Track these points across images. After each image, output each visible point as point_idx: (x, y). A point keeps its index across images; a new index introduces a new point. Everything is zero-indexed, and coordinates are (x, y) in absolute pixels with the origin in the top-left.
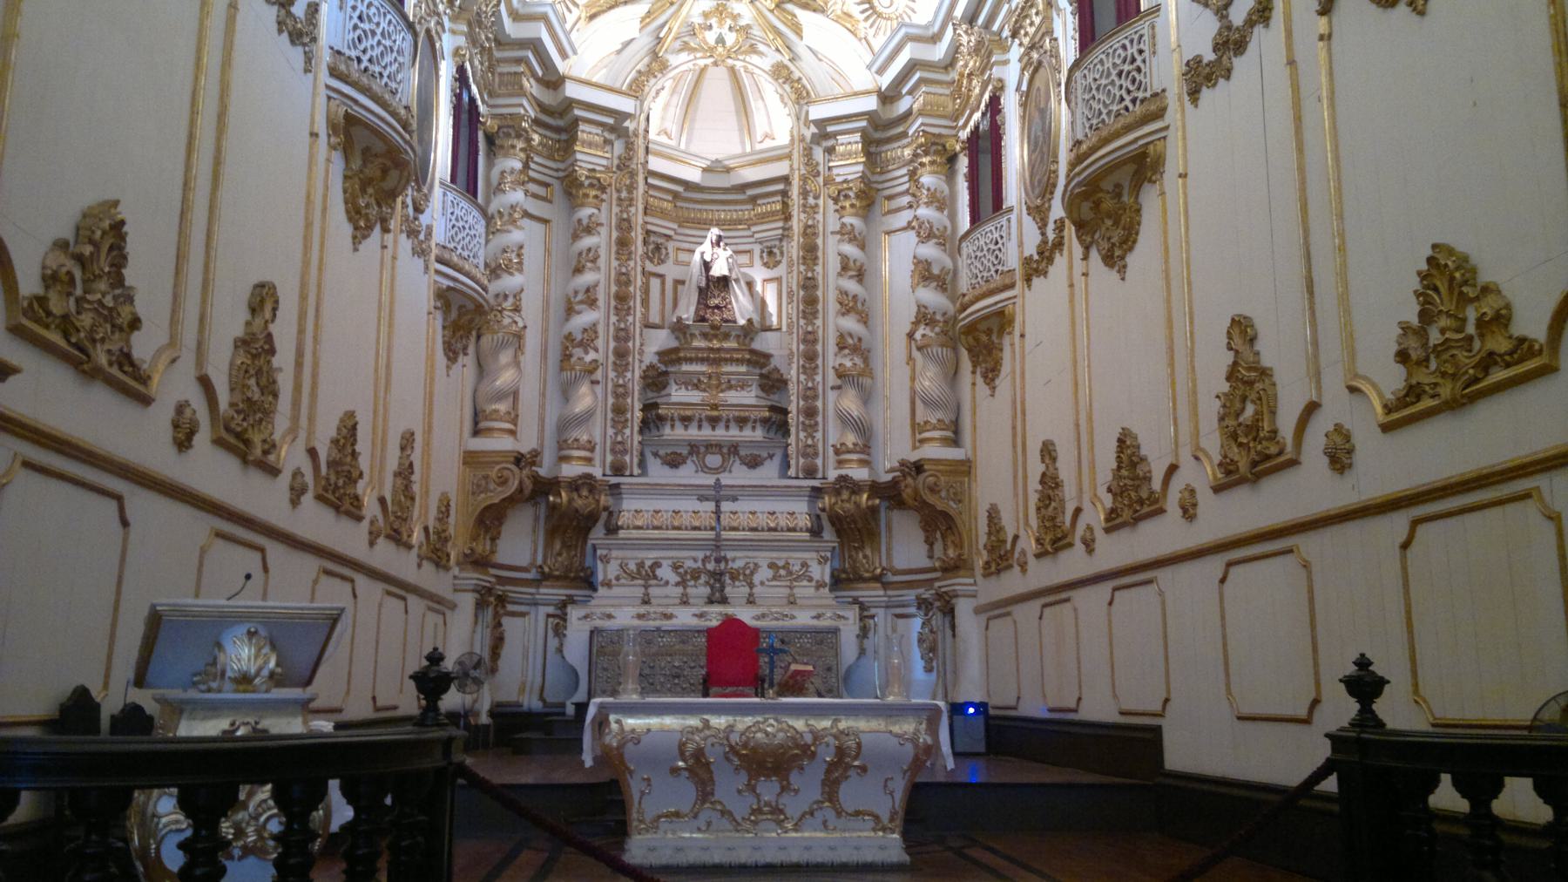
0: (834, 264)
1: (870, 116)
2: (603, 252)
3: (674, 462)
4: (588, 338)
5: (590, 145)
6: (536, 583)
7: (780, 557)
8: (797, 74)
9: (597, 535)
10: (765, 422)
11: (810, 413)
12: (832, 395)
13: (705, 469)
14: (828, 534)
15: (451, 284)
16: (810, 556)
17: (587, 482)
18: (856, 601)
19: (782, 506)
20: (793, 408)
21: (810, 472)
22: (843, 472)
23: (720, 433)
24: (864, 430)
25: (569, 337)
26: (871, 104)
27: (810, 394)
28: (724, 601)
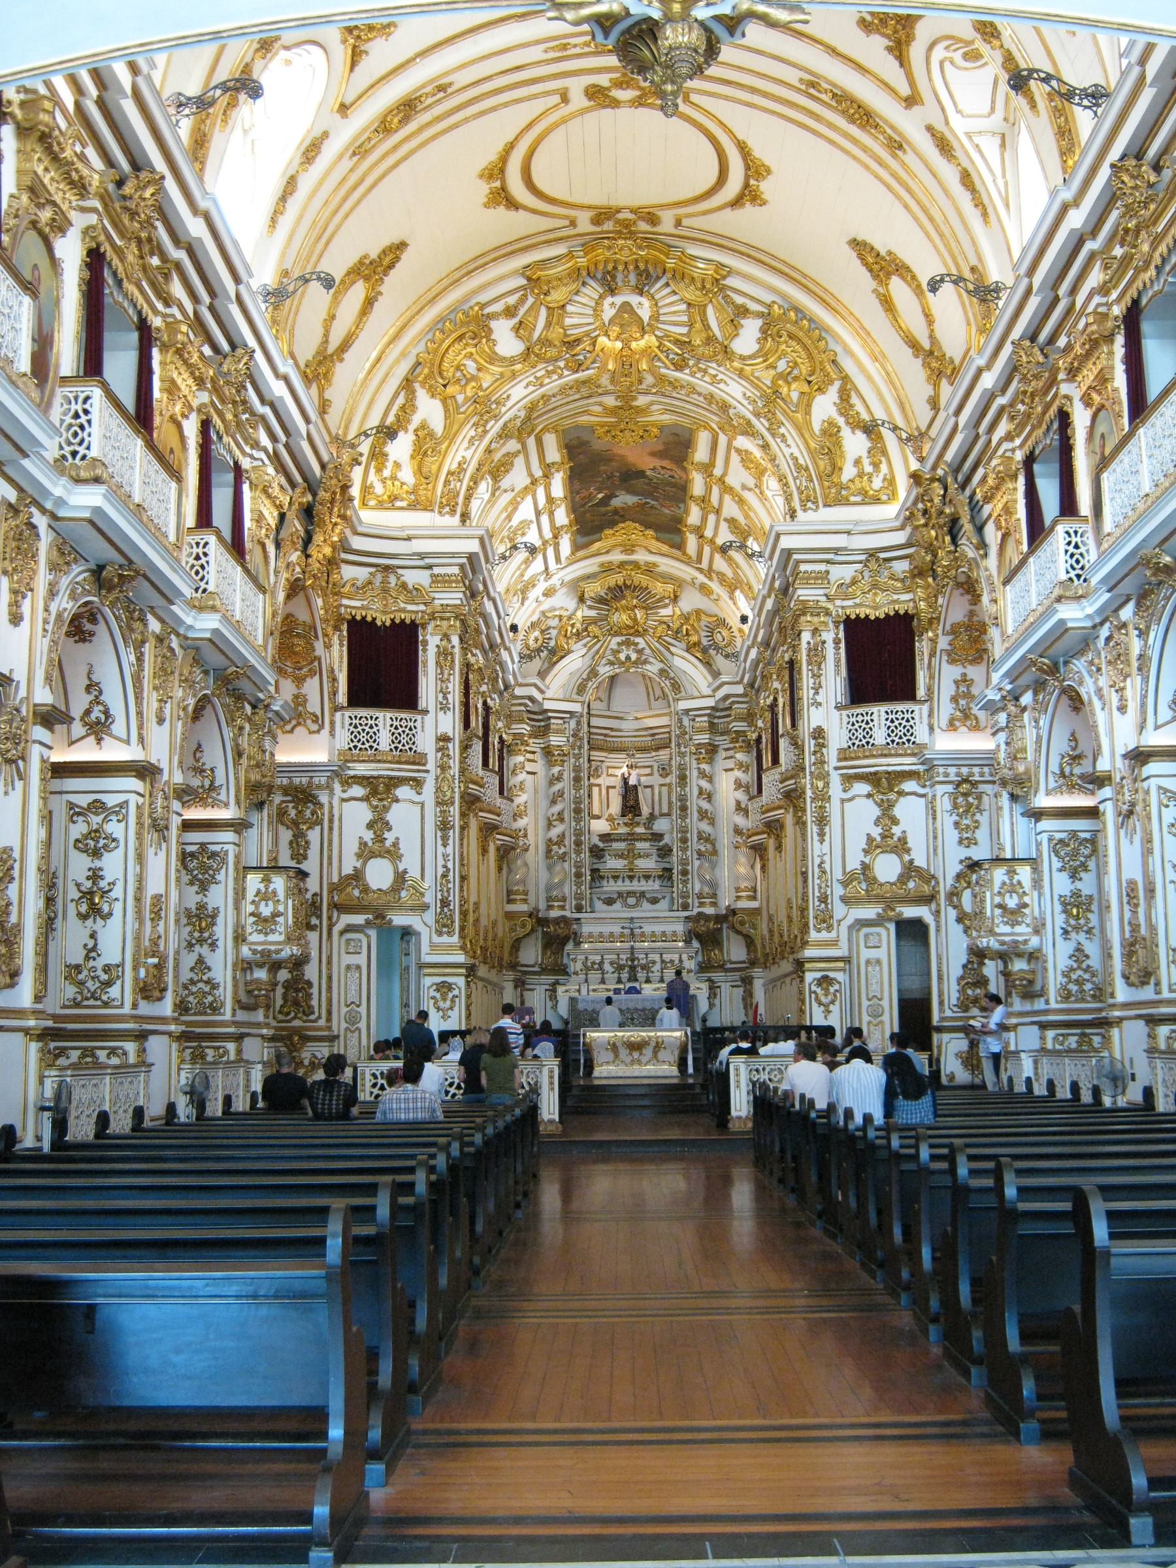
0: (696, 792)
1: (712, 708)
3: (609, 902)
5: (557, 732)
9: (569, 946)
10: (660, 877)
11: (685, 873)
14: (696, 944)
18: (709, 980)
23: (636, 886)
24: (713, 885)
25: (550, 840)
26: (711, 702)
27: (684, 862)
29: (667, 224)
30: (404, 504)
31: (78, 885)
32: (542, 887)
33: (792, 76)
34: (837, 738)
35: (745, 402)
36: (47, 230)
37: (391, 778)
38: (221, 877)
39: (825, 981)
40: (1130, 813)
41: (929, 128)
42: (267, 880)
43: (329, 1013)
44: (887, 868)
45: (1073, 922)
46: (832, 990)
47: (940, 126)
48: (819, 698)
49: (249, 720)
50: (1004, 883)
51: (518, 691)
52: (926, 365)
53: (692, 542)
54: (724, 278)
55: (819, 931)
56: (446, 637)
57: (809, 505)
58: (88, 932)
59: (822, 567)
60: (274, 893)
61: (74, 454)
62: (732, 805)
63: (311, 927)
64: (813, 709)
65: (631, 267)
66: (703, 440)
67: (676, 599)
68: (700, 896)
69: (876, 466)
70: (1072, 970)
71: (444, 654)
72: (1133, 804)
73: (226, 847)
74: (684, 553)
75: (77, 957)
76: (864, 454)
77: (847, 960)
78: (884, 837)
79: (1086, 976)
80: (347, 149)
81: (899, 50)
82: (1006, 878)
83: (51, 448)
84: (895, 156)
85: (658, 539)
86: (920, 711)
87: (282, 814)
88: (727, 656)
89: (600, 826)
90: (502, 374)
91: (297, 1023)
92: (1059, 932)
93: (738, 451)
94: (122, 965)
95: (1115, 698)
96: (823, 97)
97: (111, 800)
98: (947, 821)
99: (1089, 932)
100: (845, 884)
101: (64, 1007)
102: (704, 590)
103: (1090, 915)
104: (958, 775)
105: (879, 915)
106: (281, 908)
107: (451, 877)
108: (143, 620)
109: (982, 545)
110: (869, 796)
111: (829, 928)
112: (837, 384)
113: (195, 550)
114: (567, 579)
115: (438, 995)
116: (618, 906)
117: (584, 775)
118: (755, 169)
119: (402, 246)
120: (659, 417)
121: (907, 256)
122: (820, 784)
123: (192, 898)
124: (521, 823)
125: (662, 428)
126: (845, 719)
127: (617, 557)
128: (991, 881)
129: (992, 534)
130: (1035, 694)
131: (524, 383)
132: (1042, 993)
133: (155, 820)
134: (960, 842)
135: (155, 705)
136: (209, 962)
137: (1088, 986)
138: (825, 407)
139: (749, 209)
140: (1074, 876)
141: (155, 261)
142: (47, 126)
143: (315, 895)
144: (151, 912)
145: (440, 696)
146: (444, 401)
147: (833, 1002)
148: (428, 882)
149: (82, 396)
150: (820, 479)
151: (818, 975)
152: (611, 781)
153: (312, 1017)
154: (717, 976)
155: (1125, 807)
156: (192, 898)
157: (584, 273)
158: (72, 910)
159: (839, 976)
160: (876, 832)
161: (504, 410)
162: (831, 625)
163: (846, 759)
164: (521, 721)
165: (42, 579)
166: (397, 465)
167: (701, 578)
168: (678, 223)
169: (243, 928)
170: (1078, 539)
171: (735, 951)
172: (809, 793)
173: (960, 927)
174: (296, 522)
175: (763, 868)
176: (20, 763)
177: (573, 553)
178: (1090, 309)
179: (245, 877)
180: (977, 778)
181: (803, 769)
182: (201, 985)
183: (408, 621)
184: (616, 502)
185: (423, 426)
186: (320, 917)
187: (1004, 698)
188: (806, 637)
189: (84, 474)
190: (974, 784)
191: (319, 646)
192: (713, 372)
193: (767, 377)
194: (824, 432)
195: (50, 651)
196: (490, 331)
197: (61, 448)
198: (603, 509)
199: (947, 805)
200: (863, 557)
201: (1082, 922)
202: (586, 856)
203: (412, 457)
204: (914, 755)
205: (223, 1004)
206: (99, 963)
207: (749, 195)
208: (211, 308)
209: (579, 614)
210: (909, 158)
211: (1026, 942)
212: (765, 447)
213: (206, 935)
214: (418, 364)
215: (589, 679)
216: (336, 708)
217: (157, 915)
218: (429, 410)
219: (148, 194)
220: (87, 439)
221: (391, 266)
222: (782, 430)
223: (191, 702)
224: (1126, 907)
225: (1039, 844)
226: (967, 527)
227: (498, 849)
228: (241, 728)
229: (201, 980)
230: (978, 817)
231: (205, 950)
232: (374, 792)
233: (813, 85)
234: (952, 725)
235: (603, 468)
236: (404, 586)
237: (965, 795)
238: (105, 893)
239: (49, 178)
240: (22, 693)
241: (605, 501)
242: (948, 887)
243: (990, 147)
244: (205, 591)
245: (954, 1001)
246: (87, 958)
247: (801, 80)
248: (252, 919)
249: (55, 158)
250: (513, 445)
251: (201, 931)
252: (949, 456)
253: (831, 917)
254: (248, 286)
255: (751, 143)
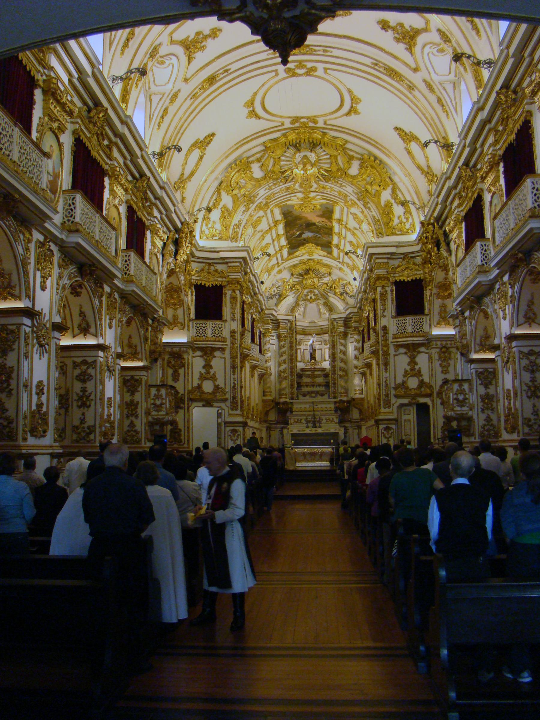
0: (339, 351)
1: (345, 318)
2: (287, 351)
3: (304, 395)
4: (284, 372)
5: (283, 328)
6: (276, 424)
7: (327, 417)
8: (329, 304)
9: (288, 414)
11: (334, 384)
12: (339, 380)
13: (311, 397)
14: (339, 412)
16: (334, 417)
17: (285, 403)
19: (328, 406)
20: (331, 383)
21: (335, 397)
22: (341, 398)
25: (280, 371)
27: (334, 380)
28: (316, 427)
29: (320, 124)
30: (217, 238)
31: (77, 394)
32: (277, 389)
33: (368, 61)
34: (393, 330)
35: (354, 194)
36: (56, 131)
37: (212, 348)
38: (139, 389)
39: (387, 429)
40: (508, 361)
41: (424, 81)
42: (158, 390)
43: (188, 441)
44: (413, 383)
45: (486, 406)
46: (390, 432)
47: (428, 80)
48: (385, 314)
49: (151, 326)
50: (457, 390)
51: (267, 312)
52: (426, 177)
53: (335, 251)
54: (344, 144)
55: (385, 408)
56: (234, 291)
57: (380, 235)
58: (81, 413)
59: (386, 260)
60: (161, 395)
61: (69, 221)
62: (354, 356)
63: (181, 408)
64: (382, 318)
65: (307, 141)
66: (337, 210)
67: (330, 274)
68: (341, 393)
69: (407, 219)
70: (485, 425)
71: (233, 298)
72: (508, 358)
73: (142, 377)
74: (333, 256)
75: (77, 423)
76: (402, 214)
77: (396, 420)
78: (412, 370)
79: (491, 428)
80: (188, 97)
81: (410, 49)
82: (458, 388)
83: (57, 219)
84: (411, 93)
85: (322, 250)
86: (426, 319)
87: (169, 362)
88: (350, 297)
89: (300, 365)
90: (255, 185)
91: (175, 446)
92: (480, 410)
93: (351, 213)
94: (94, 426)
95: (501, 315)
96: (381, 69)
97: (90, 360)
98: (437, 364)
99: (492, 410)
100: (395, 389)
101: (72, 443)
102: (340, 269)
103: (493, 403)
104: (441, 344)
105: (409, 402)
106: (164, 401)
107: (236, 387)
108: (102, 287)
109: (449, 251)
110: (405, 353)
111: (389, 407)
112: (391, 186)
113: (125, 258)
115: (232, 435)
116: (308, 397)
117: (294, 345)
118: (355, 100)
119: (213, 135)
120: (319, 201)
121: (416, 133)
122: (385, 349)
123: (128, 397)
124: (269, 364)
125: (321, 205)
126: (395, 321)
127: (306, 257)
128: (452, 389)
129: (453, 247)
130: (470, 312)
131: (264, 188)
132: (473, 435)
133: (108, 367)
134: (442, 372)
135: (108, 321)
136: (135, 424)
137: (492, 432)
138: (386, 196)
139: (353, 116)
140: (486, 387)
141: (106, 142)
142: (55, 89)
143: (182, 395)
144: (107, 404)
145: (232, 316)
146: (232, 197)
147: (390, 437)
148: (228, 389)
149: (72, 197)
150: (384, 224)
151: (385, 426)
152: (305, 347)
153: (182, 443)
154: (348, 425)
155: (506, 359)
156: (128, 397)
157: (288, 144)
158: (75, 404)
159: (393, 426)
160: (408, 368)
161: (256, 199)
162: (390, 285)
163: (396, 338)
164: (268, 324)
165: (55, 271)
166: (214, 222)
167: (340, 266)
168: (325, 123)
169: (149, 409)
170: (486, 248)
171: (355, 414)
172: (381, 352)
173: (442, 407)
174: (171, 246)
175: (365, 382)
176: (46, 346)
177: (288, 256)
178: (490, 152)
179: (149, 389)
180: (449, 346)
181: (378, 343)
182: (132, 432)
183: (218, 285)
184: (304, 236)
185: (224, 206)
186: (184, 404)
187: (457, 313)
188: (379, 289)
189: (73, 228)
190: (447, 349)
191: (183, 295)
192: (341, 183)
193: (362, 183)
194: (386, 206)
195: (59, 301)
196: (251, 167)
197: (64, 218)
198: (299, 239)
199: (437, 357)
200: (402, 256)
201: (489, 405)
202: (295, 377)
203: (220, 219)
204: (423, 336)
205: (141, 440)
206: (86, 425)
207: (352, 111)
208: (131, 161)
209: (291, 281)
210: (416, 93)
211: (467, 414)
212: (362, 212)
213: (134, 412)
214: (222, 182)
215: (295, 306)
216: (190, 320)
217: (110, 405)
218: (227, 200)
219: (101, 115)
220: (74, 215)
221: (209, 143)
222: (369, 205)
223: (124, 319)
224: (506, 401)
225: (472, 374)
226: (443, 244)
227: (259, 375)
228: (147, 329)
229: (132, 431)
230: (449, 361)
231: (133, 419)
232: (206, 354)
233: (376, 65)
234: (438, 324)
236: (216, 271)
237: (444, 353)
238: (88, 397)
239: (56, 110)
240: (47, 318)
241: (300, 235)
242: (437, 390)
243: (449, 88)
244: (129, 275)
245: (440, 437)
246: (81, 423)
247: (372, 63)
248: (152, 406)
249: (58, 102)
250: (261, 213)
251: (132, 411)
252: (435, 215)
253: (390, 403)
254: (146, 152)
255: (353, 90)
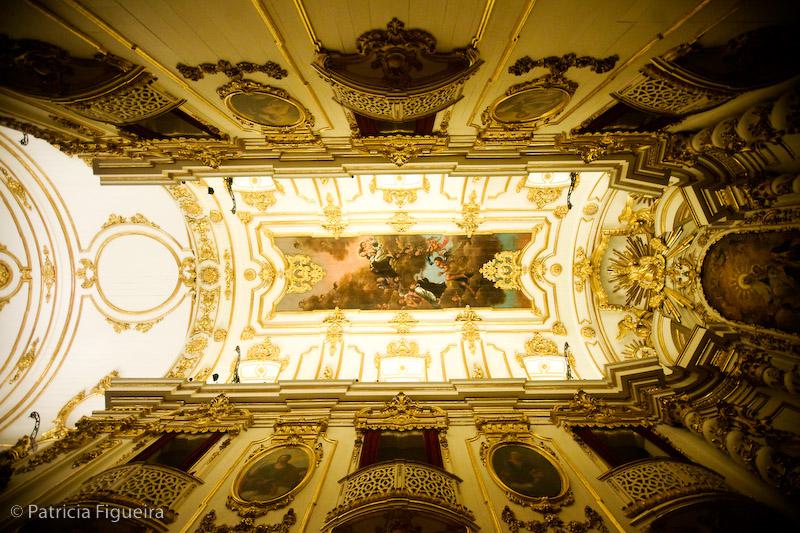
5: (724, 360)
15: (650, 521)
114: (584, 314)
235: (365, 288)
